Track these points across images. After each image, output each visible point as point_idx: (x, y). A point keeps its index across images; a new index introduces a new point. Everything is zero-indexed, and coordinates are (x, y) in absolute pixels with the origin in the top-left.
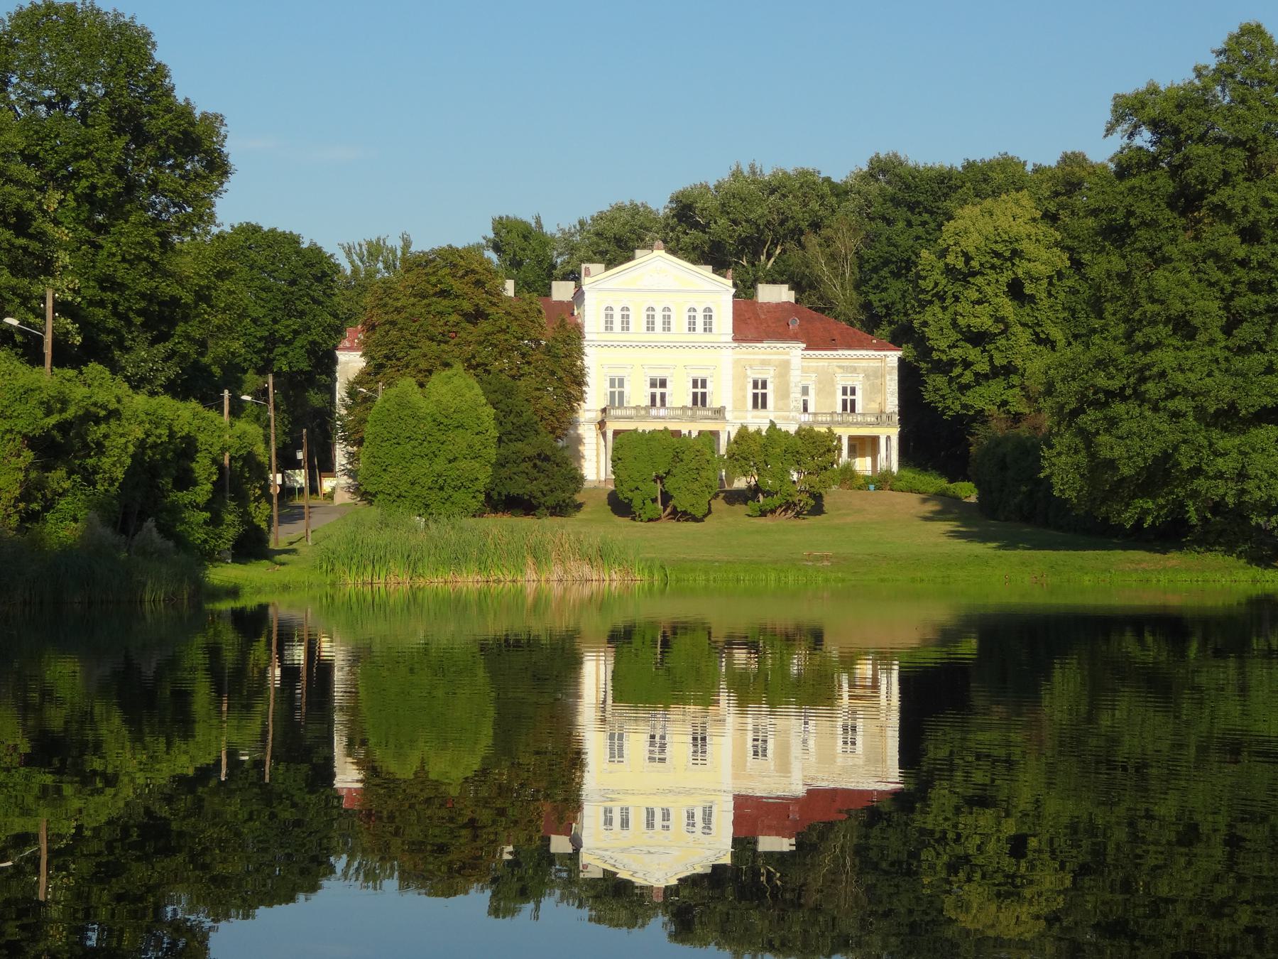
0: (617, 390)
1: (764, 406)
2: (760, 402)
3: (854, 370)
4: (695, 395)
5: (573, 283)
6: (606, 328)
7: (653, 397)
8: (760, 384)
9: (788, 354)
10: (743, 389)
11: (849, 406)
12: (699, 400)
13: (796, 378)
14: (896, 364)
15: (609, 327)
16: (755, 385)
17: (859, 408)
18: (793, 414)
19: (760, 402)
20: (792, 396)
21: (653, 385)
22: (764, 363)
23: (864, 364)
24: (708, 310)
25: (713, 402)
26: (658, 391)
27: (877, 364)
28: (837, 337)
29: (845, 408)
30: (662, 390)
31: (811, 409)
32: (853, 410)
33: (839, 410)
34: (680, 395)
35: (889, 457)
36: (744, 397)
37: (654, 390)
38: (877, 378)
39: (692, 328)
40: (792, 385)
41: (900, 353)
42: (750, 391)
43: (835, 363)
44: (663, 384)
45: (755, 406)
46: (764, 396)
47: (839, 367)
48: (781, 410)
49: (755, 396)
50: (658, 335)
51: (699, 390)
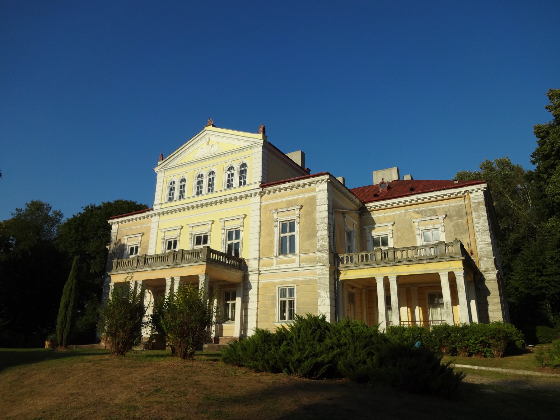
1: (292, 250)
3: (434, 212)
4: (230, 246)
8: (287, 227)
9: (314, 190)
10: (271, 234)
14: (482, 199)
16: (284, 230)
18: (319, 255)
20: (319, 233)
22: (290, 204)
23: (444, 205)
24: (244, 165)
27: (459, 202)
36: (272, 242)
38: (461, 217)
40: (318, 222)
41: (485, 185)
45: (283, 251)
46: (292, 238)
47: (417, 212)
48: (308, 251)
49: (283, 240)
50: (205, 196)
51: (234, 241)
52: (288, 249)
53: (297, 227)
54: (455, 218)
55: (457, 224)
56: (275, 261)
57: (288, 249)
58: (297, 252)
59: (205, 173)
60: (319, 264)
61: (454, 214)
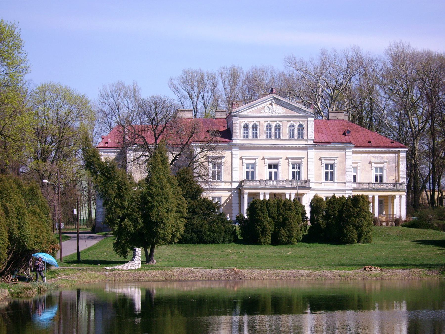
0: (250, 170)
2: (330, 177)
5: (145, 260)
6: (244, 137)
7: (270, 173)
11: (379, 179)
12: (296, 175)
13: (350, 164)
15: (246, 136)
17: (385, 180)
19: (330, 177)
21: (270, 167)
25: (303, 177)
26: (273, 171)
27: (394, 155)
28: (372, 140)
29: (376, 180)
30: (276, 170)
31: (359, 180)
32: (381, 181)
33: (374, 181)
34: (285, 173)
35: (400, 208)
37: (270, 170)
39: (292, 136)
42: (324, 170)
43: (371, 155)
44: (276, 166)
45: (327, 179)
46: (332, 173)
47: (373, 157)
49: (327, 173)
51: (296, 170)
52: (329, 178)
53: (336, 169)
54: (391, 163)
55: (392, 166)
56: (323, 184)
57: (329, 178)
58: (336, 181)
59: (274, 125)
60: (347, 188)
61: (391, 160)
